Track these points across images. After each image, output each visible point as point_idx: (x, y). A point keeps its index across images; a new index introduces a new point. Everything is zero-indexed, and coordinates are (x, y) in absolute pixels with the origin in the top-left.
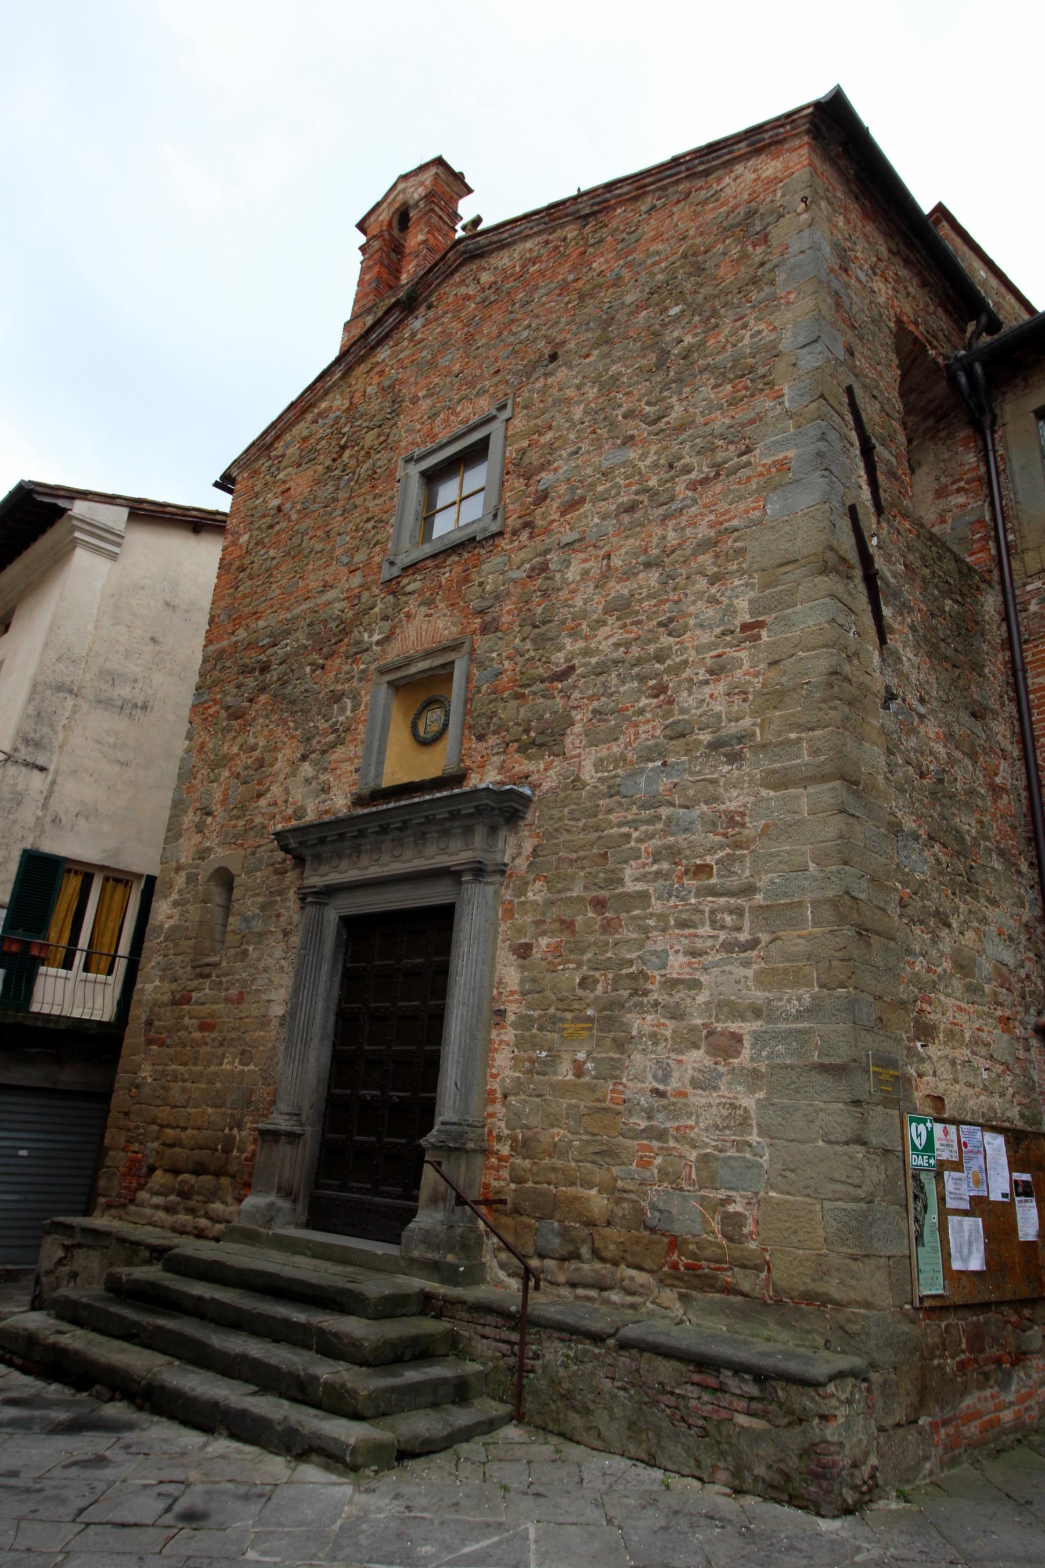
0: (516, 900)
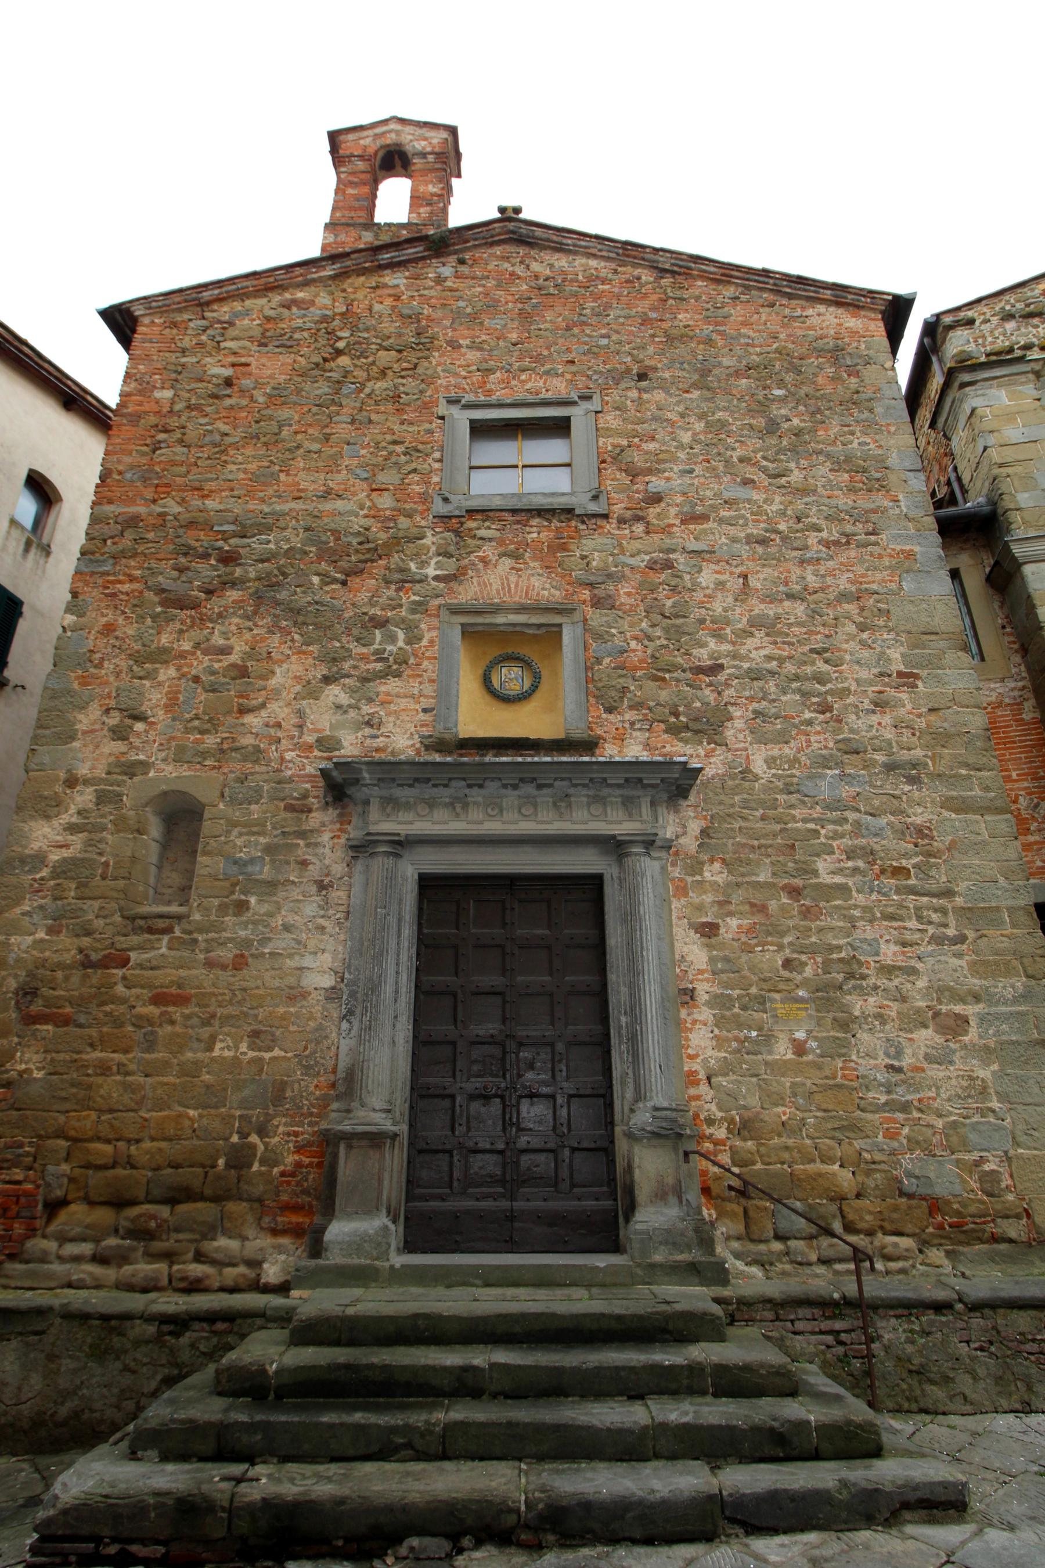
0: (689, 879)
